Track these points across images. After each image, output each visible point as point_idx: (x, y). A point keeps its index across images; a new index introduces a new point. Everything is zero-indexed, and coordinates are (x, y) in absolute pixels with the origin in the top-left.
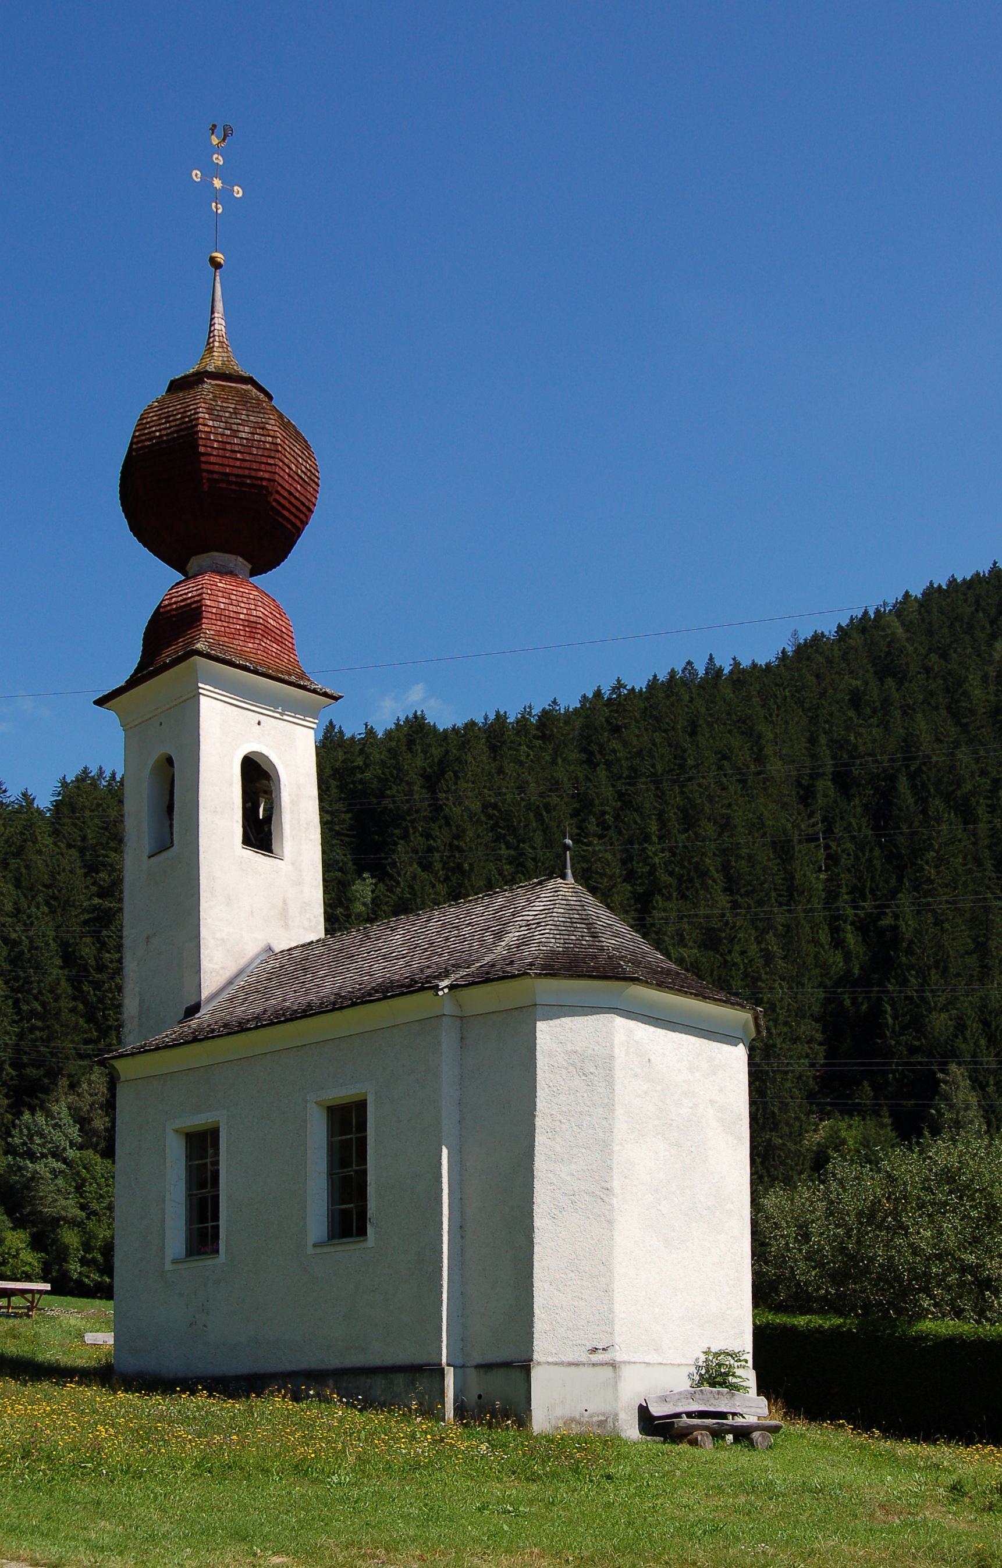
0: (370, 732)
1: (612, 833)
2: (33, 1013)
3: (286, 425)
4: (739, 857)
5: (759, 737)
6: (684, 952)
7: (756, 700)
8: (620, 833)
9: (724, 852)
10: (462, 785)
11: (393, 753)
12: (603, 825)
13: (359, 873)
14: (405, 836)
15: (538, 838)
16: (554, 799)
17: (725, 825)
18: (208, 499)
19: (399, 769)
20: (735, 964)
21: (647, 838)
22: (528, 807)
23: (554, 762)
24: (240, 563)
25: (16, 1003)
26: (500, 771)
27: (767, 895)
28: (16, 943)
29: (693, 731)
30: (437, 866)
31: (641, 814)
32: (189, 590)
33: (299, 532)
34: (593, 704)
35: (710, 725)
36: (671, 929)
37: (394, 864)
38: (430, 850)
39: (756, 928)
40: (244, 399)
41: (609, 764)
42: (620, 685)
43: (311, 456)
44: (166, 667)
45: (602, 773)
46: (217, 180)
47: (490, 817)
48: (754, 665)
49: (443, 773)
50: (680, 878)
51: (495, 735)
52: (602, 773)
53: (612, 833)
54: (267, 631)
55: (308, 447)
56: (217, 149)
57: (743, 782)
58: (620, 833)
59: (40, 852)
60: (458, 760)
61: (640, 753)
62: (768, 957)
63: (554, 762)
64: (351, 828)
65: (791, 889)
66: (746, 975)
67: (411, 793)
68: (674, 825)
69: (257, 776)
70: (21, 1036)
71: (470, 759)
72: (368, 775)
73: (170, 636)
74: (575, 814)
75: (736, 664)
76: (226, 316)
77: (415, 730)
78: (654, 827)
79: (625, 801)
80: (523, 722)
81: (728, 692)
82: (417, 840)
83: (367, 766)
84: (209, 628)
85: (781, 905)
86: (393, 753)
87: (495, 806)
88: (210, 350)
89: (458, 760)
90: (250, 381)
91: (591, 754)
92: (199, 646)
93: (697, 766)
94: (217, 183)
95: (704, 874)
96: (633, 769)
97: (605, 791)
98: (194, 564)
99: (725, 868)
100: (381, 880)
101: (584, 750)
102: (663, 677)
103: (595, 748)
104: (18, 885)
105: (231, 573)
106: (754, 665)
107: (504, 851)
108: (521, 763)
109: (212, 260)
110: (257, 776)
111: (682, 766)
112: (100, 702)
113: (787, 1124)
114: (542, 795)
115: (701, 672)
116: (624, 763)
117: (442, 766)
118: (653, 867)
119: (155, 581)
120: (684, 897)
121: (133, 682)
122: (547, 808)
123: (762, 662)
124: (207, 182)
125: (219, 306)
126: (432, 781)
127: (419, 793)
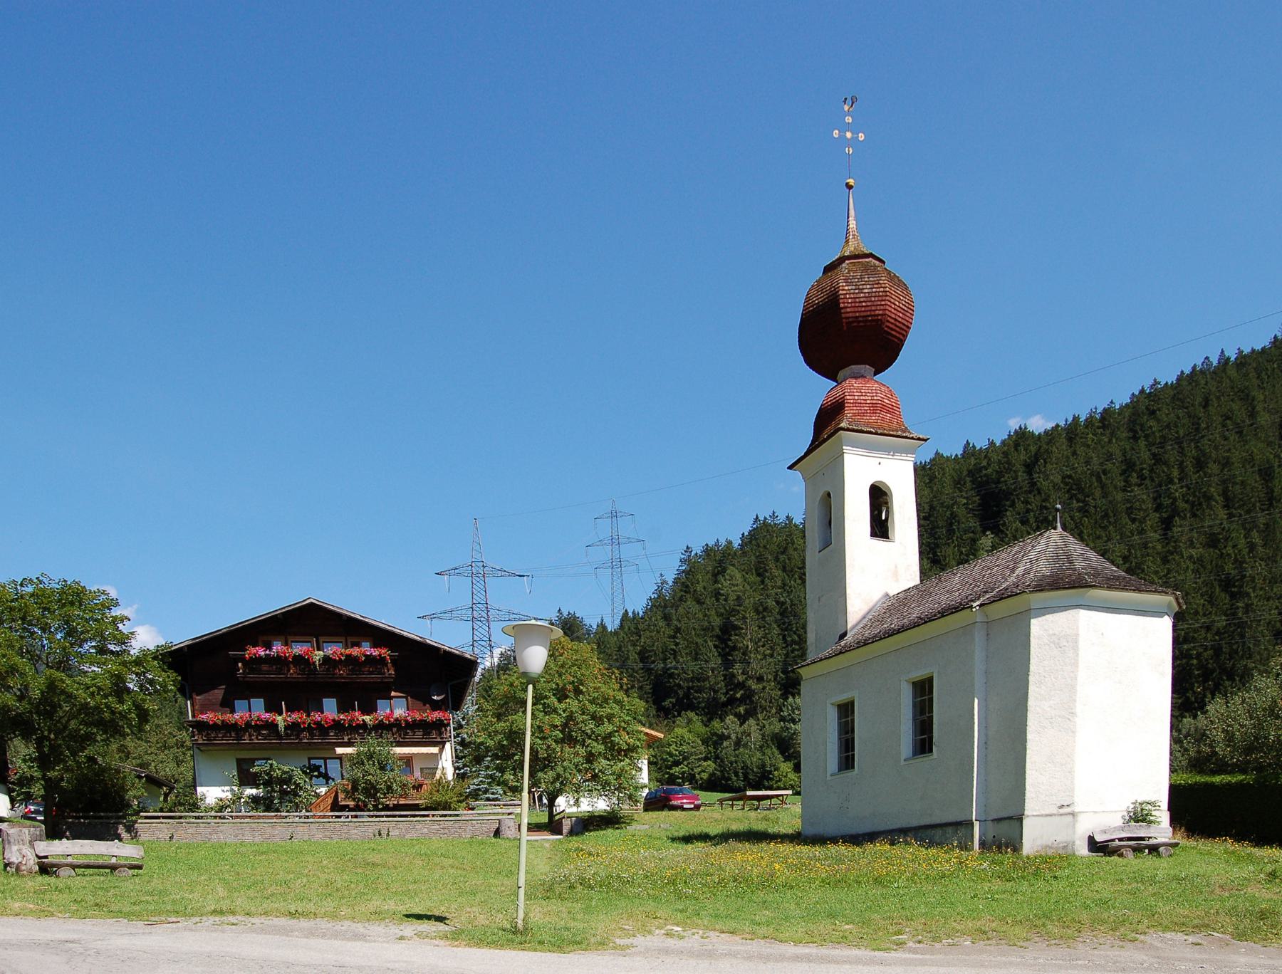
0: (992, 443)
1: (1148, 482)
2: (793, 642)
3: (892, 277)
4: (1235, 484)
5: (1253, 399)
6: (1193, 552)
7: (1252, 374)
8: (1153, 480)
9: (1224, 482)
10: (1049, 466)
11: (1005, 454)
12: (1142, 478)
13: (984, 533)
14: (1013, 505)
15: (1098, 493)
16: (1109, 466)
17: (1226, 464)
18: (848, 336)
19: (1009, 463)
20: (1228, 555)
21: (1171, 481)
22: (1092, 474)
23: (1110, 441)
24: (868, 369)
25: (784, 638)
26: (1074, 453)
27: (1254, 505)
28: (783, 603)
29: (1206, 403)
30: (1032, 520)
31: (1168, 466)
32: (838, 393)
33: (902, 343)
34: (1136, 400)
35: (1218, 398)
36: (1184, 538)
37: (1004, 524)
38: (1028, 511)
39: (1245, 529)
40: (866, 267)
41: (1147, 436)
42: (1156, 382)
43: (909, 294)
44: (825, 440)
45: (1142, 443)
46: (849, 134)
47: (1067, 484)
48: (1253, 351)
49: (1037, 460)
50: (1193, 504)
51: (1072, 433)
52: (1142, 443)
53: (1148, 482)
54: (884, 408)
55: (906, 288)
56: (849, 113)
57: (1240, 433)
58: (1153, 480)
59: (796, 549)
60: (1047, 451)
61: (1168, 426)
62: (1252, 547)
63: (1110, 441)
64: (979, 505)
65: (1270, 499)
66: (1236, 560)
67: (1016, 477)
68: (1190, 469)
69: (879, 496)
70: (787, 655)
71: (1054, 449)
72: (990, 470)
73: (828, 421)
74: (1124, 472)
75: (1240, 351)
76: (856, 219)
77: (1022, 436)
78: (1175, 473)
79: (1157, 459)
80: (1090, 421)
81: (1232, 373)
82: (1020, 506)
83: (989, 465)
84: (848, 412)
85: (1263, 510)
86: (1005, 454)
87: (1070, 477)
88: (847, 242)
89: (1047, 451)
90: (871, 255)
91: (1135, 432)
92: (843, 425)
93: (1207, 428)
94: (849, 135)
95: (1209, 498)
96: (1163, 437)
97: (1143, 454)
98: (841, 375)
99: (1225, 493)
100: (997, 535)
101: (1131, 430)
102: (1187, 372)
103: (1138, 428)
104: (784, 570)
105: (863, 376)
106: (1253, 351)
107: (1075, 504)
108: (1088, 446)
109: (847, 184)
110: (879, 496)
111: (1197, 430)
112: (790, 468)
113: (1259, 653)
114: (1101, 464)
115: (1215, 363)
116: (1157, 435)
117: (1036, 457)
118: (1175, 499)
119: (819, 389)
120: (1194, 515)
121: (807, 454)
122: (1105, 472)
123: (1258, 347)
124: (842, 137)
125: (852, 212)
126: (1029, 468)
127: (1022, 476)
